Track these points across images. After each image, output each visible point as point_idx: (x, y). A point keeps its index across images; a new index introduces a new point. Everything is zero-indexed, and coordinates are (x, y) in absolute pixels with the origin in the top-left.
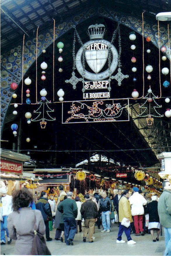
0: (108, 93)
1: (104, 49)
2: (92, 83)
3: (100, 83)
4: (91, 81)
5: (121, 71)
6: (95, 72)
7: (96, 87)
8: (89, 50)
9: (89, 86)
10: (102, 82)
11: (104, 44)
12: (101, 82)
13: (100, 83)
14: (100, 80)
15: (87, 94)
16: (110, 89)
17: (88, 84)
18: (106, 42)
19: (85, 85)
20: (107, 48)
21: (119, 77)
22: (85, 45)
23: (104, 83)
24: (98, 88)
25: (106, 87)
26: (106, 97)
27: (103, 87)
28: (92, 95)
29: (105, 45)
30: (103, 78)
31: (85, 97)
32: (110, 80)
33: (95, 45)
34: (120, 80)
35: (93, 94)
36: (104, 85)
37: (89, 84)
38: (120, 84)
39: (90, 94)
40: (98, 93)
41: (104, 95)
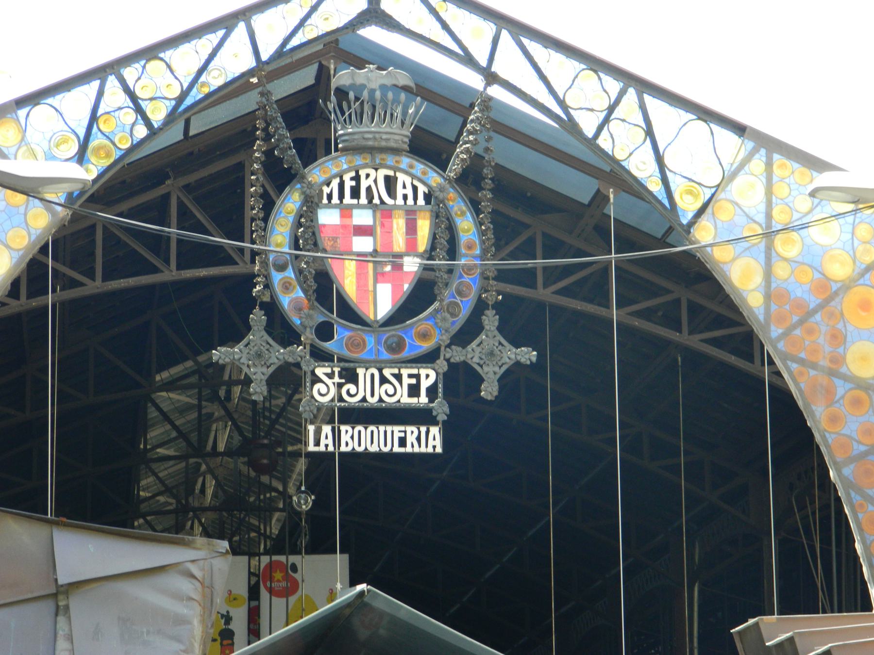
0: (435, 430)
1: (410, 201)
2: (351, 377)
3: (394, 375)
4: (347, 365)
5: (496, 324)
6: (368, 321)
7: (372, 395)
8: (335, 200)
9: (340, 386)
10: (405, 372)
11: (413, 177)
12: (396, 371)
13: (394, 375)
14: (392, 363)
15: (327, 429)
16: (441, 408)
17: (330, 376)
18: (419, 167)
19: (316, 380)
20: (428, 197)
21: (491, 354)
22: (316, 174)
23: (410, 376)
24: (381, 400)
25: (424, 399)
26: (423, 449)
27: (406, 400)
28: (352, 437)
29: (416, 183)
30: (406, 354)
31: (317, 443)
32: (442, 365)
33: (368, 176)
34: (495, 373)
35: (360, 432)
36: (410, 386)
37: (337, 379)
38: (489, 390)
39: (343, 428)
40: (382, 428)
41: (411, 439)
